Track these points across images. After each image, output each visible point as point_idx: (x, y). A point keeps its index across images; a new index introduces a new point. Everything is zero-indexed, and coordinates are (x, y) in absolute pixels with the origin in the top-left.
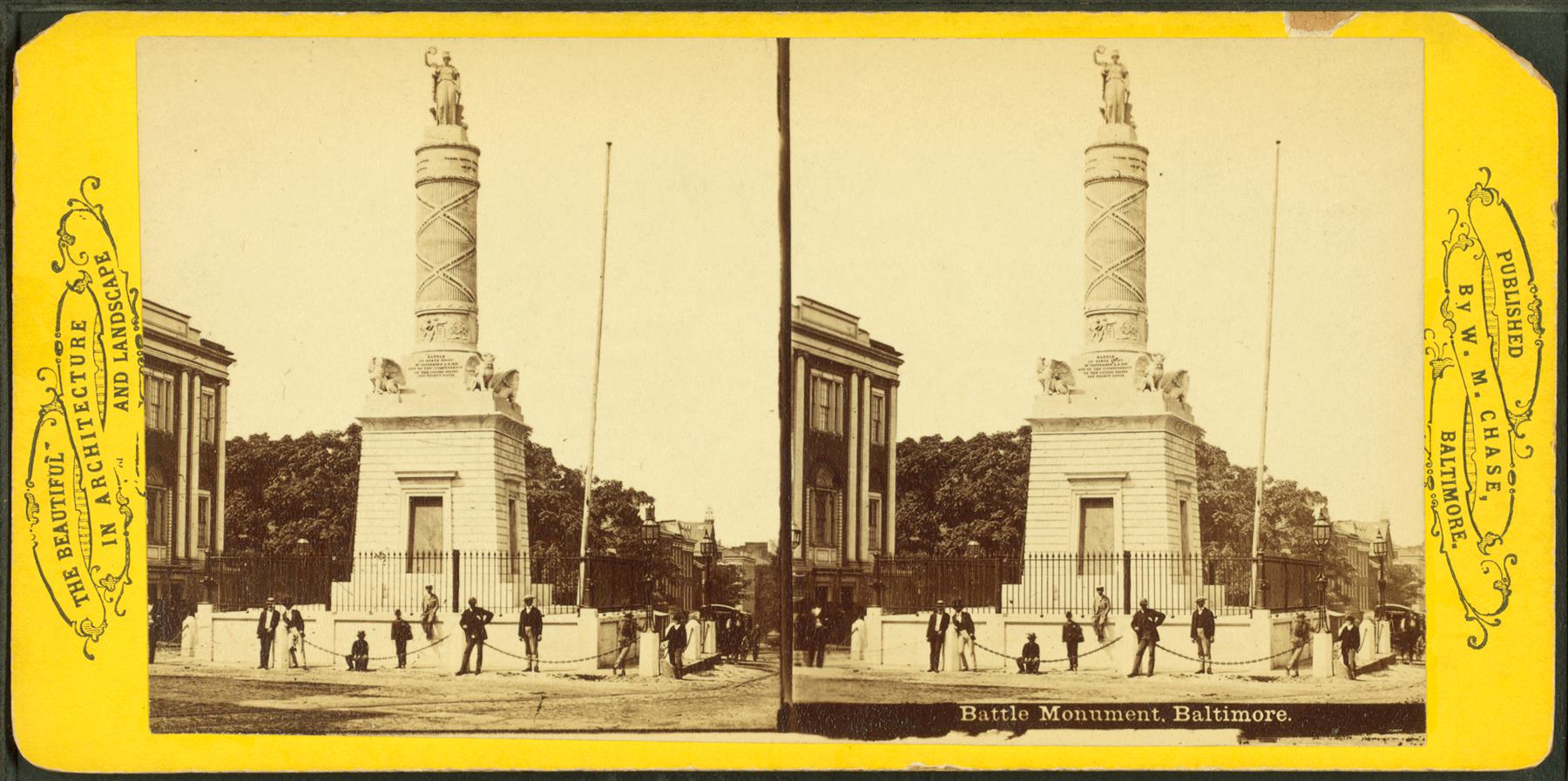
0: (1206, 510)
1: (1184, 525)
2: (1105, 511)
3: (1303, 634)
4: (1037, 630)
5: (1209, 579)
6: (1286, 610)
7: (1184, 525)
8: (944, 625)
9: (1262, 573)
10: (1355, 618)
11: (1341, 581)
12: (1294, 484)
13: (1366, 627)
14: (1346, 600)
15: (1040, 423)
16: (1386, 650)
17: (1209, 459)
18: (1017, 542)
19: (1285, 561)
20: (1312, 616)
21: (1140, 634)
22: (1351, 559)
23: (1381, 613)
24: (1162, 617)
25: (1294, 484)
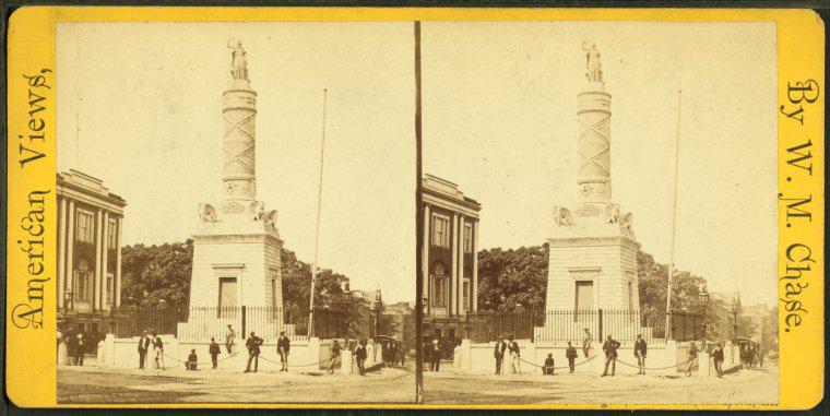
0: (285, 284)
1: (274, 293)
2: (231, 284)
3: (336, 350)
4: (197, 348)
5: (287, 321)
6: (327, 338)
7: (274, 293)
8: (147, 345)
9: (315, 319)
10: (364, 343)
11: (355, 323)
12: (331, 271)
13: (369, 347)
14: (358, 332)
15: (199, 238)
16: (379, 359)
17: (287, 258)
18: (185, 301)
19: (326, 311)
20: (341, 341)
21: (250, 350)
22: (360, 310)
23: (377, 340)
24: (262, 341)
25: (331, 271)
